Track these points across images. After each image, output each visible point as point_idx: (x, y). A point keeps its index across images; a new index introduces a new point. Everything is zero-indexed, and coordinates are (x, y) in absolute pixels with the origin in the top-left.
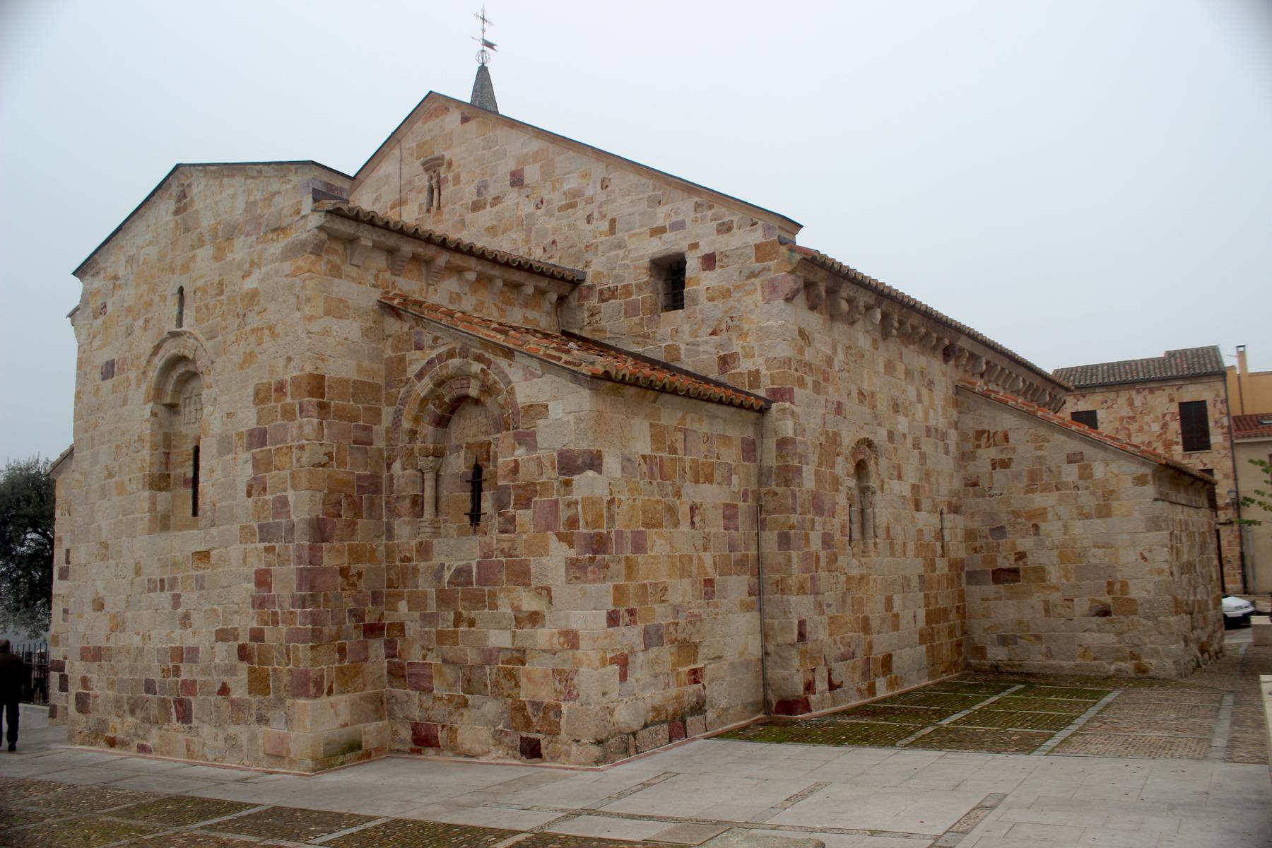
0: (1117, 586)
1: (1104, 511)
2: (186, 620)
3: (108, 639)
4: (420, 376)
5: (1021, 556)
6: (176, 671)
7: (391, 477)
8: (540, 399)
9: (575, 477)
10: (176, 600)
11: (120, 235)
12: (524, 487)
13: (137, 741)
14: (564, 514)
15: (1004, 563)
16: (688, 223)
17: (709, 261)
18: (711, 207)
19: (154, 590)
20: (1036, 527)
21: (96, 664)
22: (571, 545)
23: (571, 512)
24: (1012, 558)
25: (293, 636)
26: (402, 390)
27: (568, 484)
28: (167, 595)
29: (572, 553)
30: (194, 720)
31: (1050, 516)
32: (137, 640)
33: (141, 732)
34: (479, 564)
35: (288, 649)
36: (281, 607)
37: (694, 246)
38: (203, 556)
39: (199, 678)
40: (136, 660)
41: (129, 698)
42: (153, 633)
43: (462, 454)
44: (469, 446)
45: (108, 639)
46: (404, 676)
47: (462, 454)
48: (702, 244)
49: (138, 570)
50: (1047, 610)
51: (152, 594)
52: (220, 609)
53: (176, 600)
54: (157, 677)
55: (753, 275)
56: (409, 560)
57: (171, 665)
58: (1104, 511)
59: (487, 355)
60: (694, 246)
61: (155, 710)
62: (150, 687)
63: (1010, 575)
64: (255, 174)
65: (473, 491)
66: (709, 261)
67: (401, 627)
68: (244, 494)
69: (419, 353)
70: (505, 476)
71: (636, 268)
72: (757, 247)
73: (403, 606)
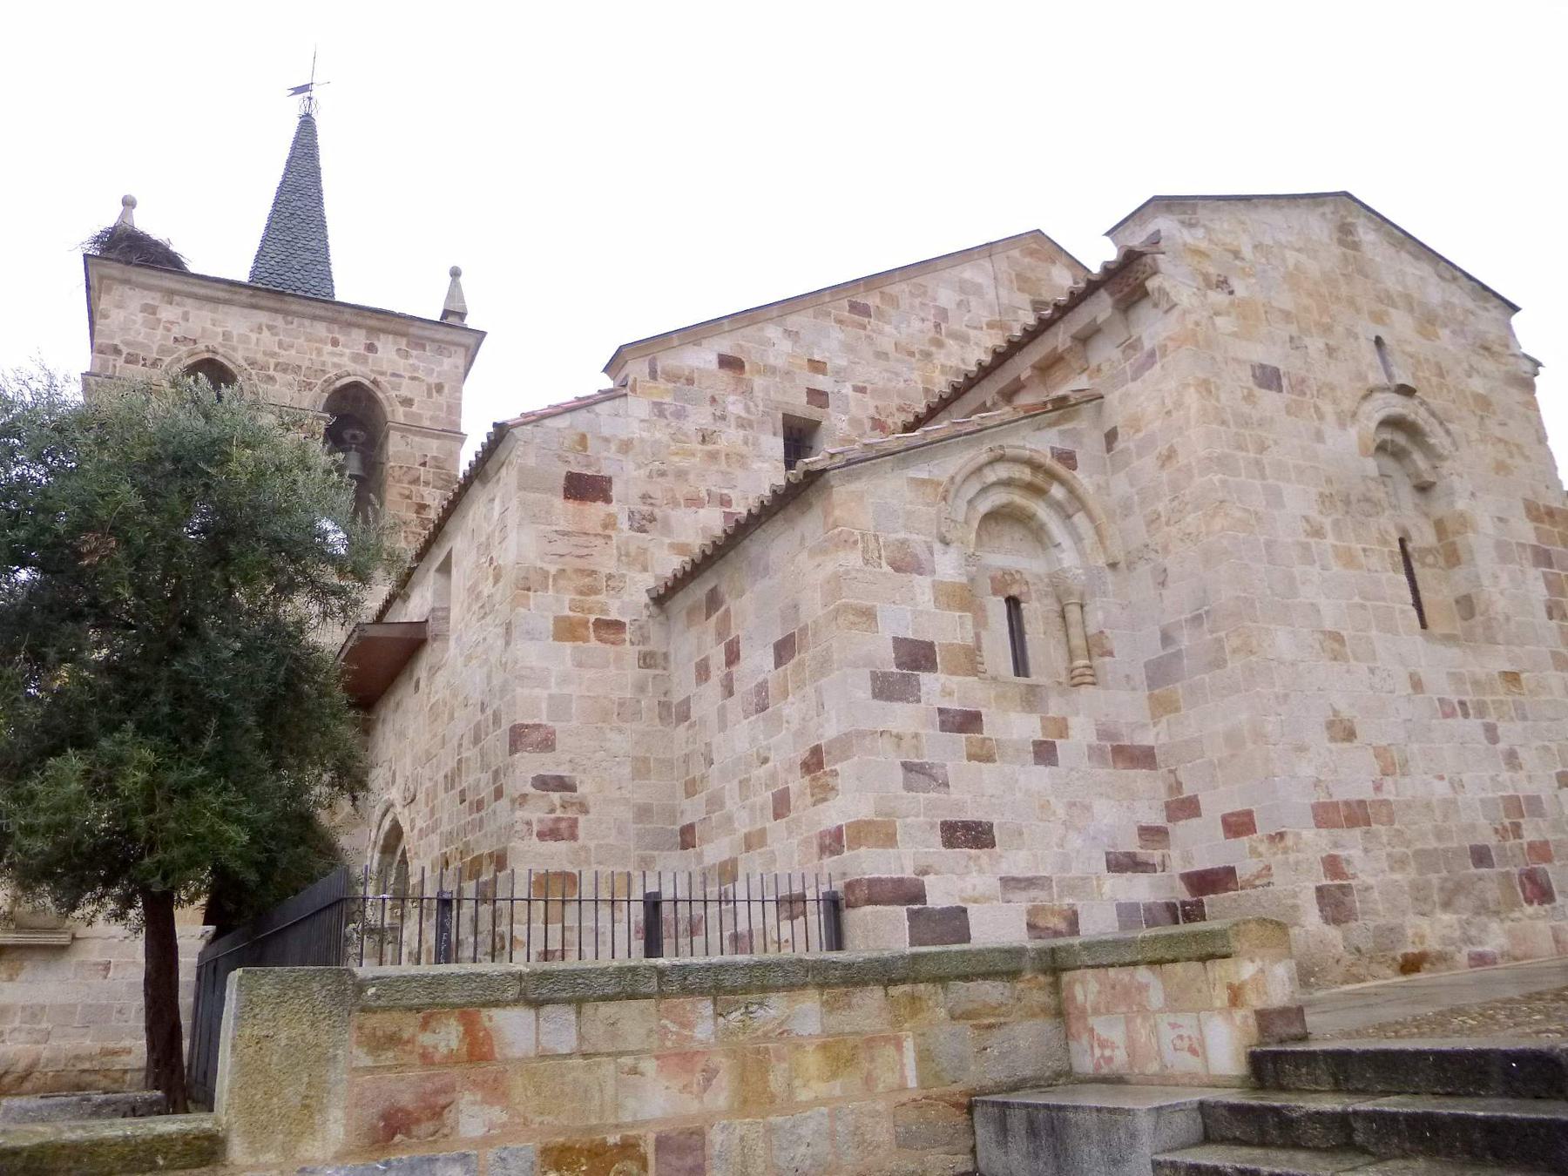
2: (1512, 759)
3: (1378, 788)
6: (1516, 830)
10: (1491, 733)
11: (1241, 205)
13: (1466, 950)
19: (1452, 714)
21: (1357, 832)
28: (1474, 725)
30: (1557, 897)
32: (1442, 789)
33: (1473, 932)
38: (1512, 678)
39: (1551, 837)
40: (1446, 817)
42: (1465, 778)
45: (1378, 788)
49: (1417, 685)
51: (1449, 721)
52: (1554, 746)
53: (1491, 733)
54: (1492, 841)
57: (1507, 822)
61: (1493, 892)
62: (1481, 856)
64: (1448, 275)
68: (1544, 614)
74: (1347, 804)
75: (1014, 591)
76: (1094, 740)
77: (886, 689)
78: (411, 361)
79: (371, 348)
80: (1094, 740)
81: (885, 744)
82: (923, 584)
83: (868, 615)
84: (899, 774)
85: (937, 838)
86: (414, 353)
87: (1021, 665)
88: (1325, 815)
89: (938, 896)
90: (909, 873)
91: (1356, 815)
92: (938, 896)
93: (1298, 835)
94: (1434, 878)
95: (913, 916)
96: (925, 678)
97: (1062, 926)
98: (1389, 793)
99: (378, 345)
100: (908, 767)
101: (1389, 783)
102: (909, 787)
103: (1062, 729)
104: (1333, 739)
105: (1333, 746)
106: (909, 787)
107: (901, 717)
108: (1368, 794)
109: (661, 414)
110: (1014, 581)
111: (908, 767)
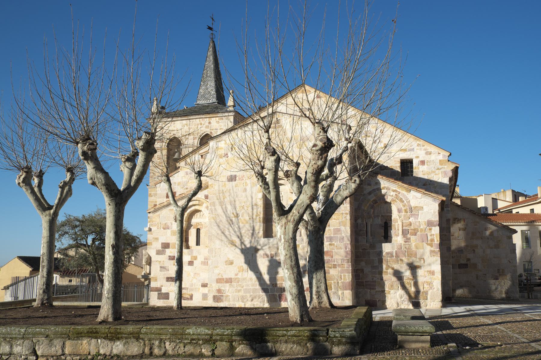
0: (501, 271)
1: (497, 246)
4: (370, 193)
5: (468, 260)
7: (357, 224)
8: (421, 205)
9: (433, 228)
12: (414, 229)
14: (429, 238)
15: (463, 262)
16: (415, 149)
17: (423, 163)
18: (423, 146)
20: (474, 250)
21: (228, 284)
22: (432, 246)
23: (432, 237)
24: (465, 260)
25: (342, 272)
26: (362, 197)
27: (430, 229)
29: (432, 249)
31: (479, 247)
34: (396, 251)
35: (341, 275)
36: (337, 262)
37: (417, 157)
41: (251, 295)
43: (380, 218)
44: (382, 216)
46: (363, 285)
47: (380, 218)
48: (420, 157)
50: (477, 278)
55: (438, 169)
56: (366, 249)
58: (497, 246)
59: (398, 190)
60: (417, 157)
63: (465, 266)
65: (385, 230)
66: (423, 163)
67: (362, 271)
69: (369, 187)
70: (406, 226)
71: (395, 161)
72: (440, 161)
73: (363, 264)
74: (226, 278)
75: (198, 227)
76: (203, 260)
77: (158, 253)
78: (220, 124)
79: (210, 123)
80: (203, 260)
81: (158, 263)
82: (169, 231)
83: (157, 239)
84: (159, 268)
85: (165, 280)
86: (220, 121)
87: (198, 243)
88: (219, 281)
89: (164, 291)
90: (159, 286)
91: (229, 281)
92: (164, 291)
93: (211, 285)
94: (248, 295)
95: (159, 294)
96: (167, 250)
97: (189, 297)
98: (240, 276)
99: (211, 121)
100: (161, 267)
101: (240, 274)
102: (161, 271)
103: (196, 258)
104: (226, 265)
105: (226, 266)
106: (161, 271)
107: (161, 258)
108: (233, 276)
109: (187, 174)
110: (199, 225)
111: (161, 267)
